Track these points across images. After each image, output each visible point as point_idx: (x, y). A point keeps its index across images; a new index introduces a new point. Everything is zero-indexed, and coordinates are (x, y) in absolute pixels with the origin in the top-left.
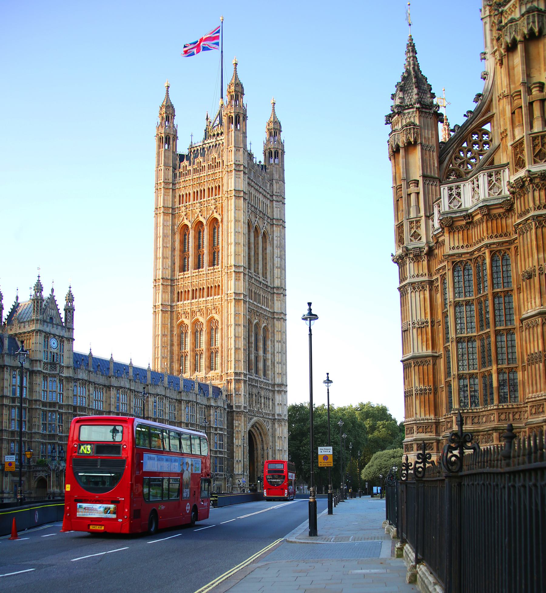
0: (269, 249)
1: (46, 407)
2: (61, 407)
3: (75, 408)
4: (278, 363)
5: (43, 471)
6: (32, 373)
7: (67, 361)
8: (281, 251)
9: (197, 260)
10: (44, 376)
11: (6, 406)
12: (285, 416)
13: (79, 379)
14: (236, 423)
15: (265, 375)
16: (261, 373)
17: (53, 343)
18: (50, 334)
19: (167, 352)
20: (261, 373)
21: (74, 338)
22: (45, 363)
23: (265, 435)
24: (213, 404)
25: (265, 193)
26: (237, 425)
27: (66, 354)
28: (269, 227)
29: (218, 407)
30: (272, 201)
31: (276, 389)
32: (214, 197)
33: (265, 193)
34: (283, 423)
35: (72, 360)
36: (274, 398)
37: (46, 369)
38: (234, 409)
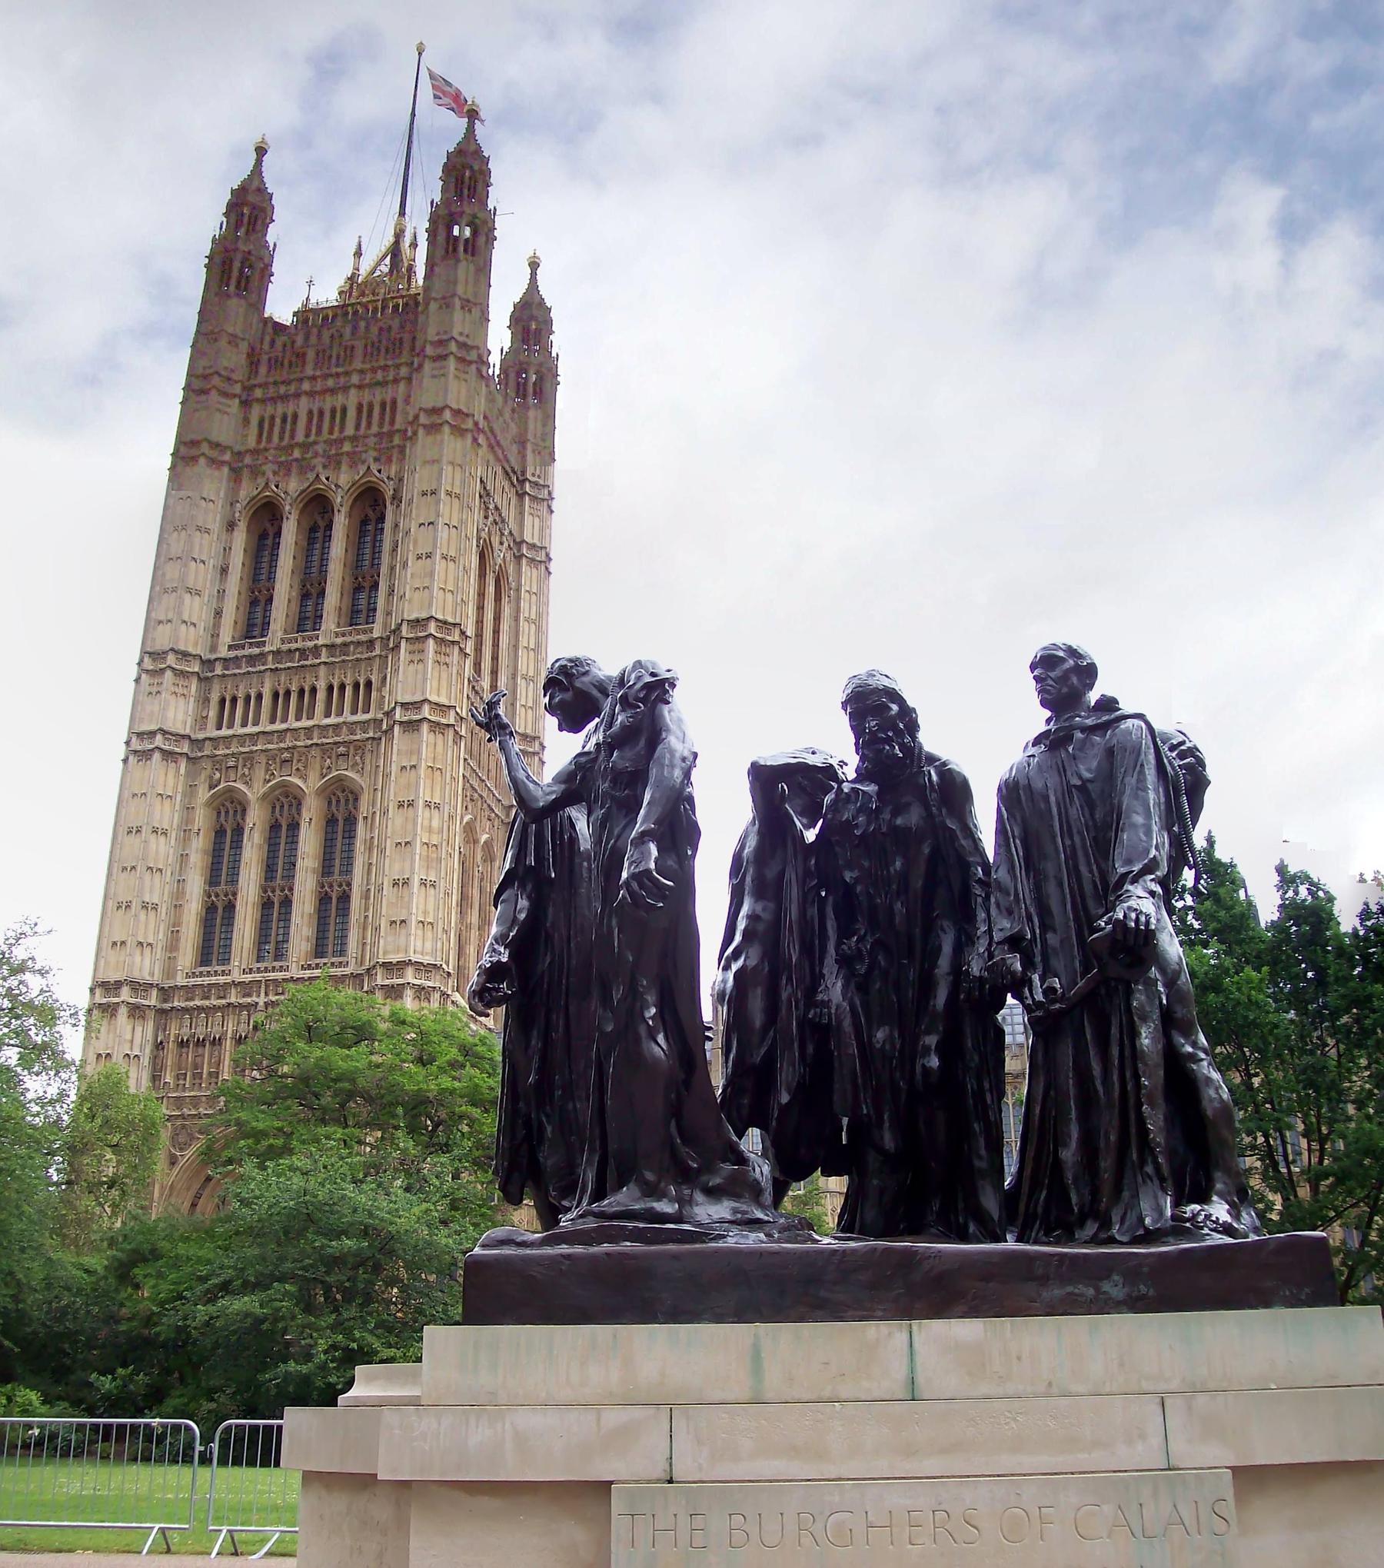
30: (521, 496)
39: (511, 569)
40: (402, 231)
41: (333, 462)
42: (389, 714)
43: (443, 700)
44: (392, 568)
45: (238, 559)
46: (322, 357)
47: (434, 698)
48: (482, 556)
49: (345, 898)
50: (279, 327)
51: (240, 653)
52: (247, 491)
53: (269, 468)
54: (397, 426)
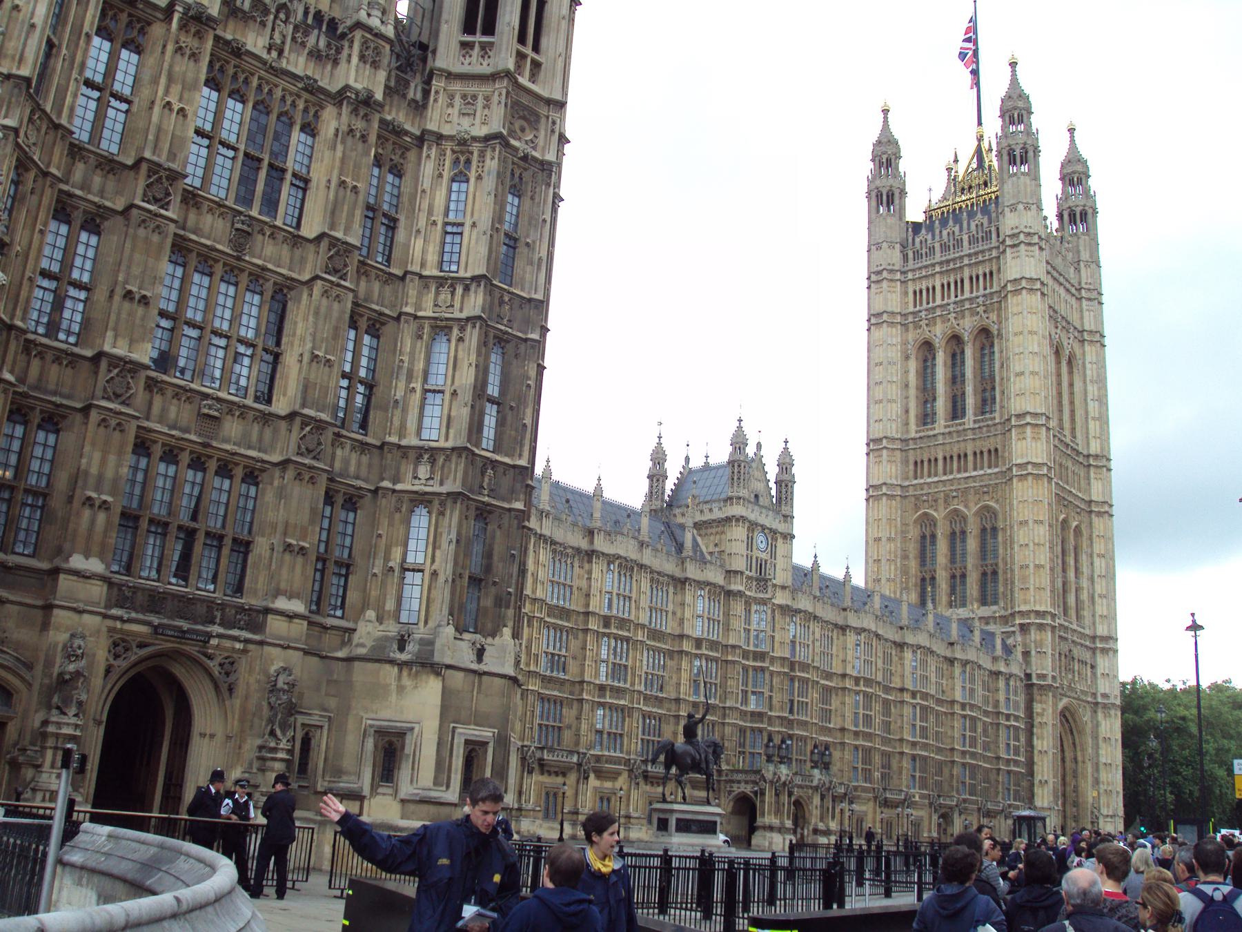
0: (1078, 385)
1: (748, 659)
2: (773, 659)
3: (792, 666)
4: (1100, 596)
5: (746, 782)
6: (729, 593)
7: (781, 577)
8: (1099, 389)
9: (950, 405)
10: (746, 602)
11: (687, 653)
12: (1116, 697)
13: (800, 611)
14: (1037, 708)
15: (1078, 617)
16: (1073, 613)
17: (760, 540)
18: (757, 524)
19: (896, 569)
20: (1073, 613)
21: (795, 533)
22: (749, 578)
23: (1079, 732)
24: (1002, 669)
25: (1068, 286)
26: (1039, 710)
27: (780, 563)
28: (1076, 346)
29: (1011, 675)
30: (1079, 299)
31: (1099, 645)
32: (982, 292)
33: (1068, 286)
34: (1112, 712)
35: (790, 574)
36: (1095, 661)
37: (750, 589)
38: (1035, 681)
39: (1078, 352)
40: (982, 136)
41: (960, 315)
42: (1010, 469)
43: (1040, 461)
44: (1002, 379)
45: (912, 378)
46: (945, 248)
47: (1034, 460)
48: (1057, 353)
49: (995, 573)
50: (916, 227)
51: (922, 434)
52: (911, 336)
53: (923, 323)
54: (995, 288)
